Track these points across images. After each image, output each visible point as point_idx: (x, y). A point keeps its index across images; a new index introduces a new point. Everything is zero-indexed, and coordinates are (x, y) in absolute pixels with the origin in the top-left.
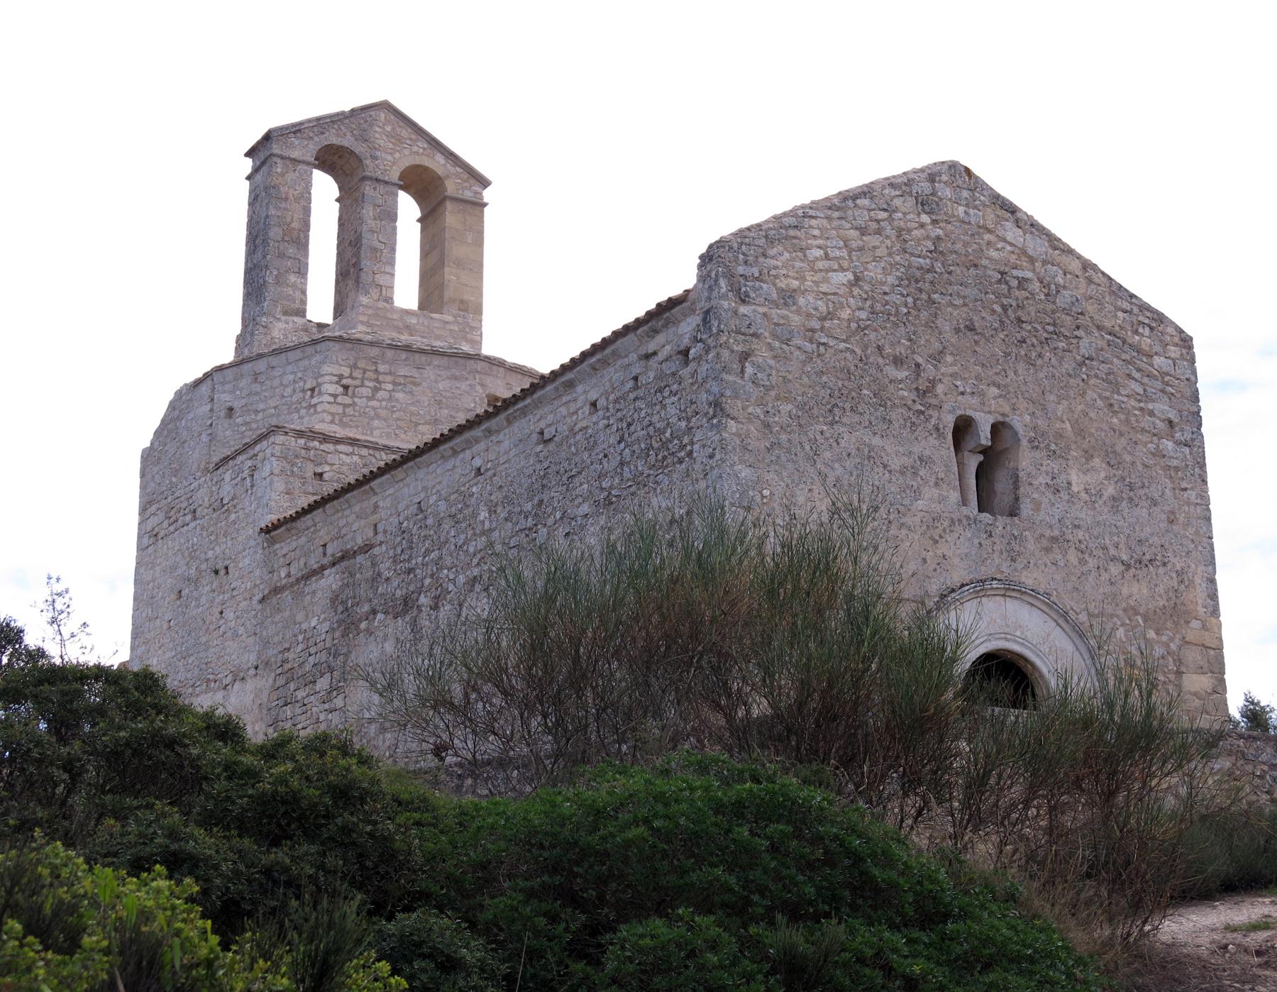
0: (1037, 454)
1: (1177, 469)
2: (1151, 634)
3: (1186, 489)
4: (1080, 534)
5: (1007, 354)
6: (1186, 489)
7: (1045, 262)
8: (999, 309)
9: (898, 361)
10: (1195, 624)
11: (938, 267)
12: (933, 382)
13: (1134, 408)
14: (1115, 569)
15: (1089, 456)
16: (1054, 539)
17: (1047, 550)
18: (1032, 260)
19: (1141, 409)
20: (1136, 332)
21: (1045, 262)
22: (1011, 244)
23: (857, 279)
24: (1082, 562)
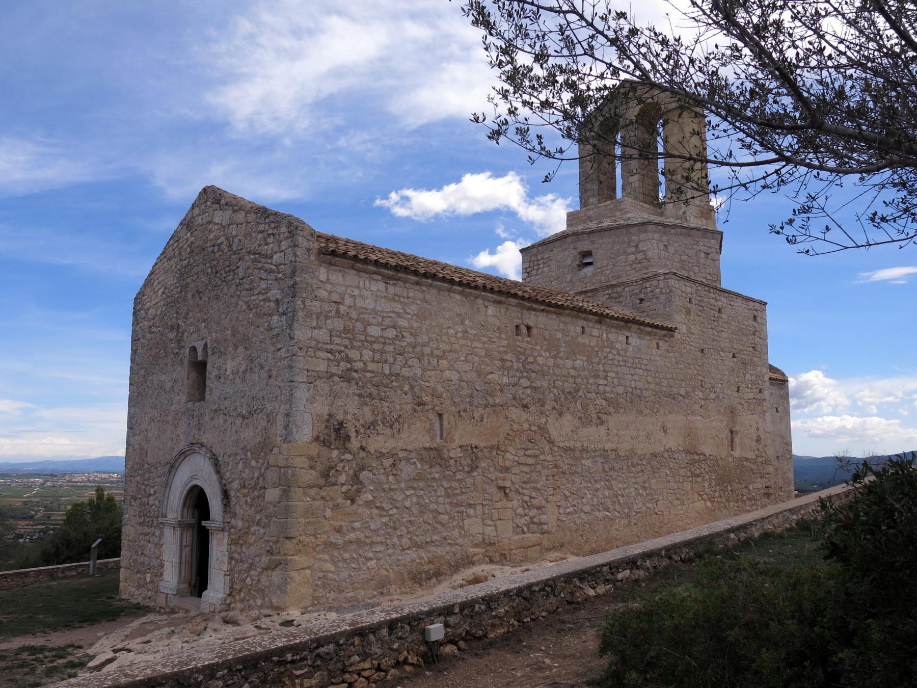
0: (214, 357)
1: (278, 335)
2: (254, 463)
3: (280, 349)
4: (227, 403)
5: (209, 298)
6: (280, 349)
7: (229, 225)
8: (209, 270)
9: (172, 328)
10: (276, 450)
11: (192, 260)
12: (183, 333)
13: (261, 301)
14: (239, 421)
15: (236, 347)
16: (216, 411)
17: (212, 419)
18: (224, 227)
19: (264, 300)
20: (267, 244)
21: (229, 225)
22: (217, 224)
23: (165, 288)
24: (225, 421)
